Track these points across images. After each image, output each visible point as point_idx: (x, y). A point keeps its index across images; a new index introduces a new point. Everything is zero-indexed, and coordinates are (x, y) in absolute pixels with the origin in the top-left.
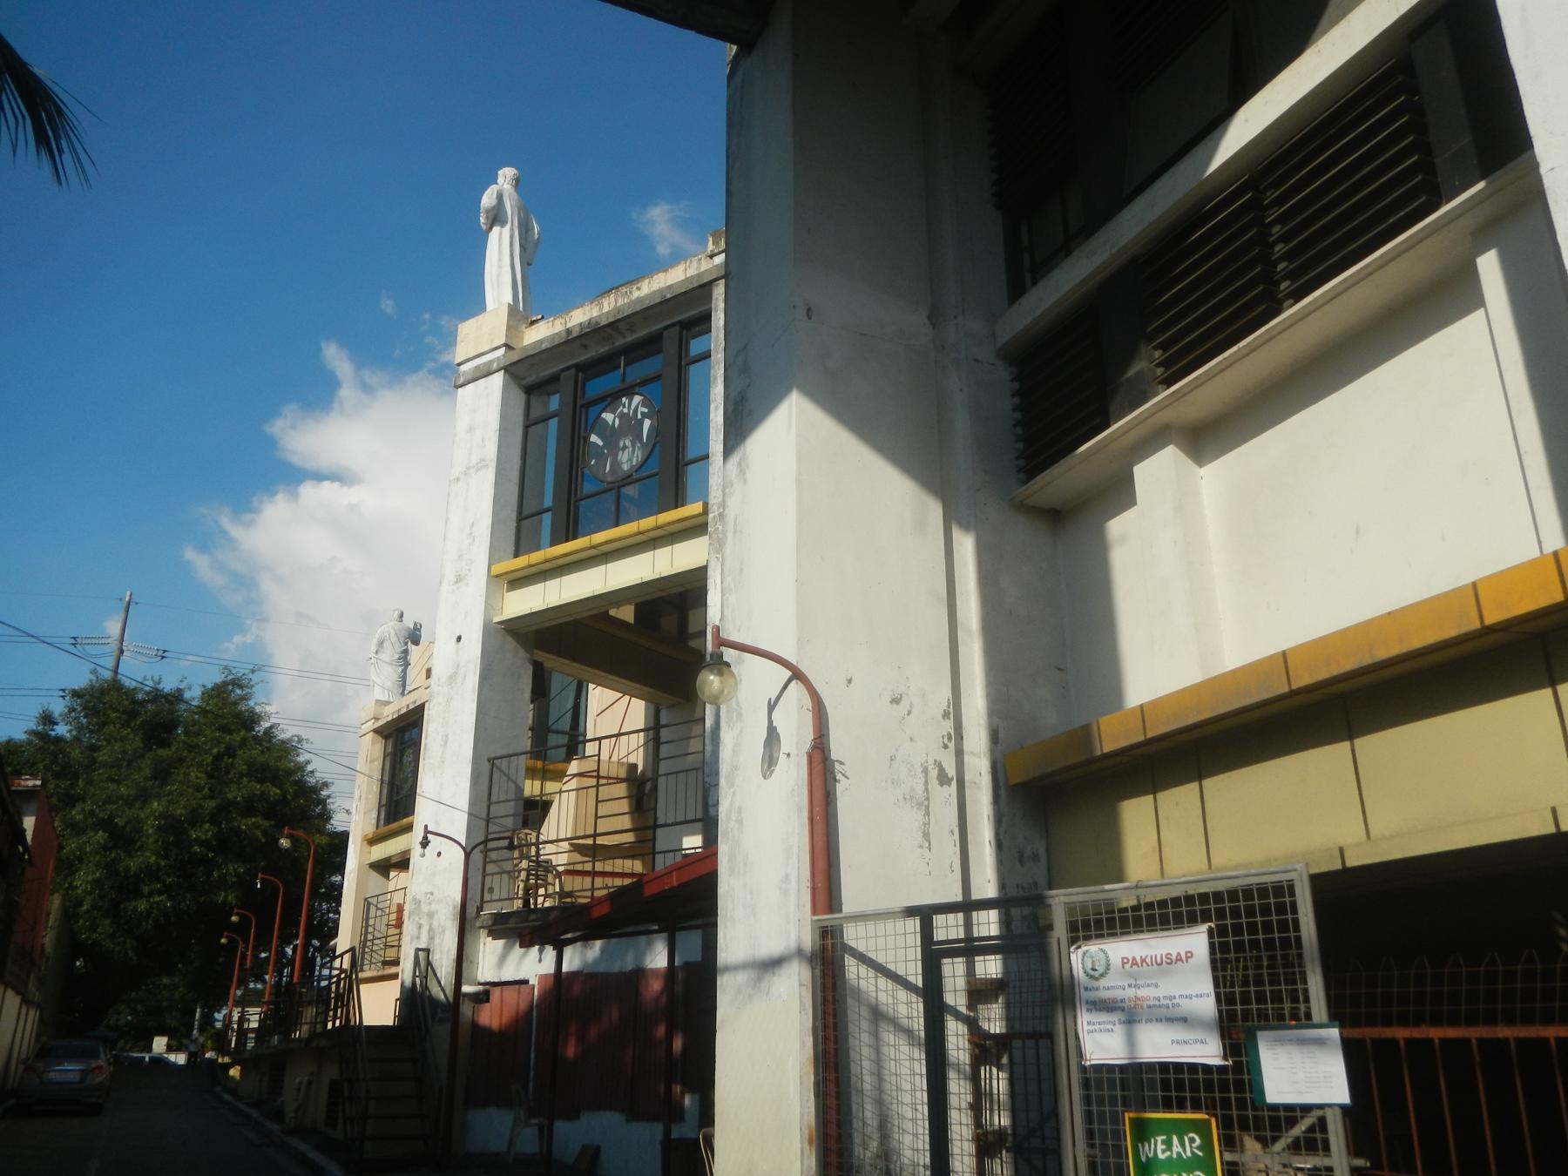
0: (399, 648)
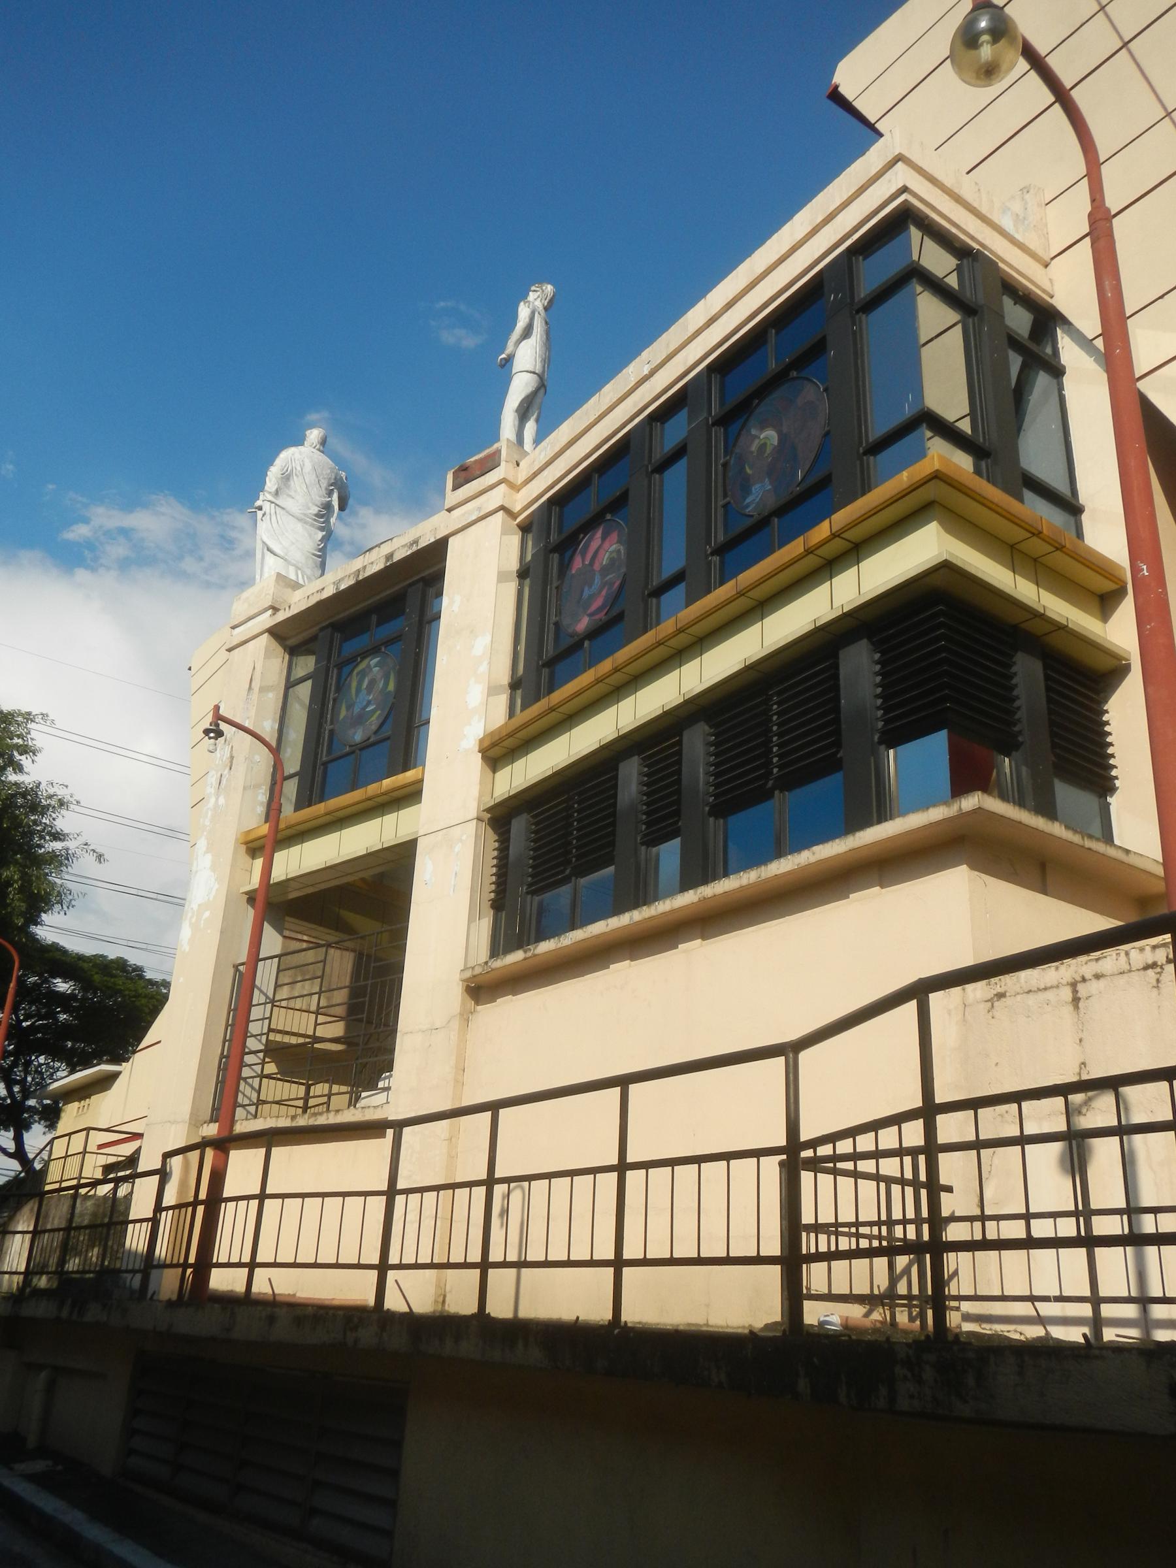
0: (318, 496)
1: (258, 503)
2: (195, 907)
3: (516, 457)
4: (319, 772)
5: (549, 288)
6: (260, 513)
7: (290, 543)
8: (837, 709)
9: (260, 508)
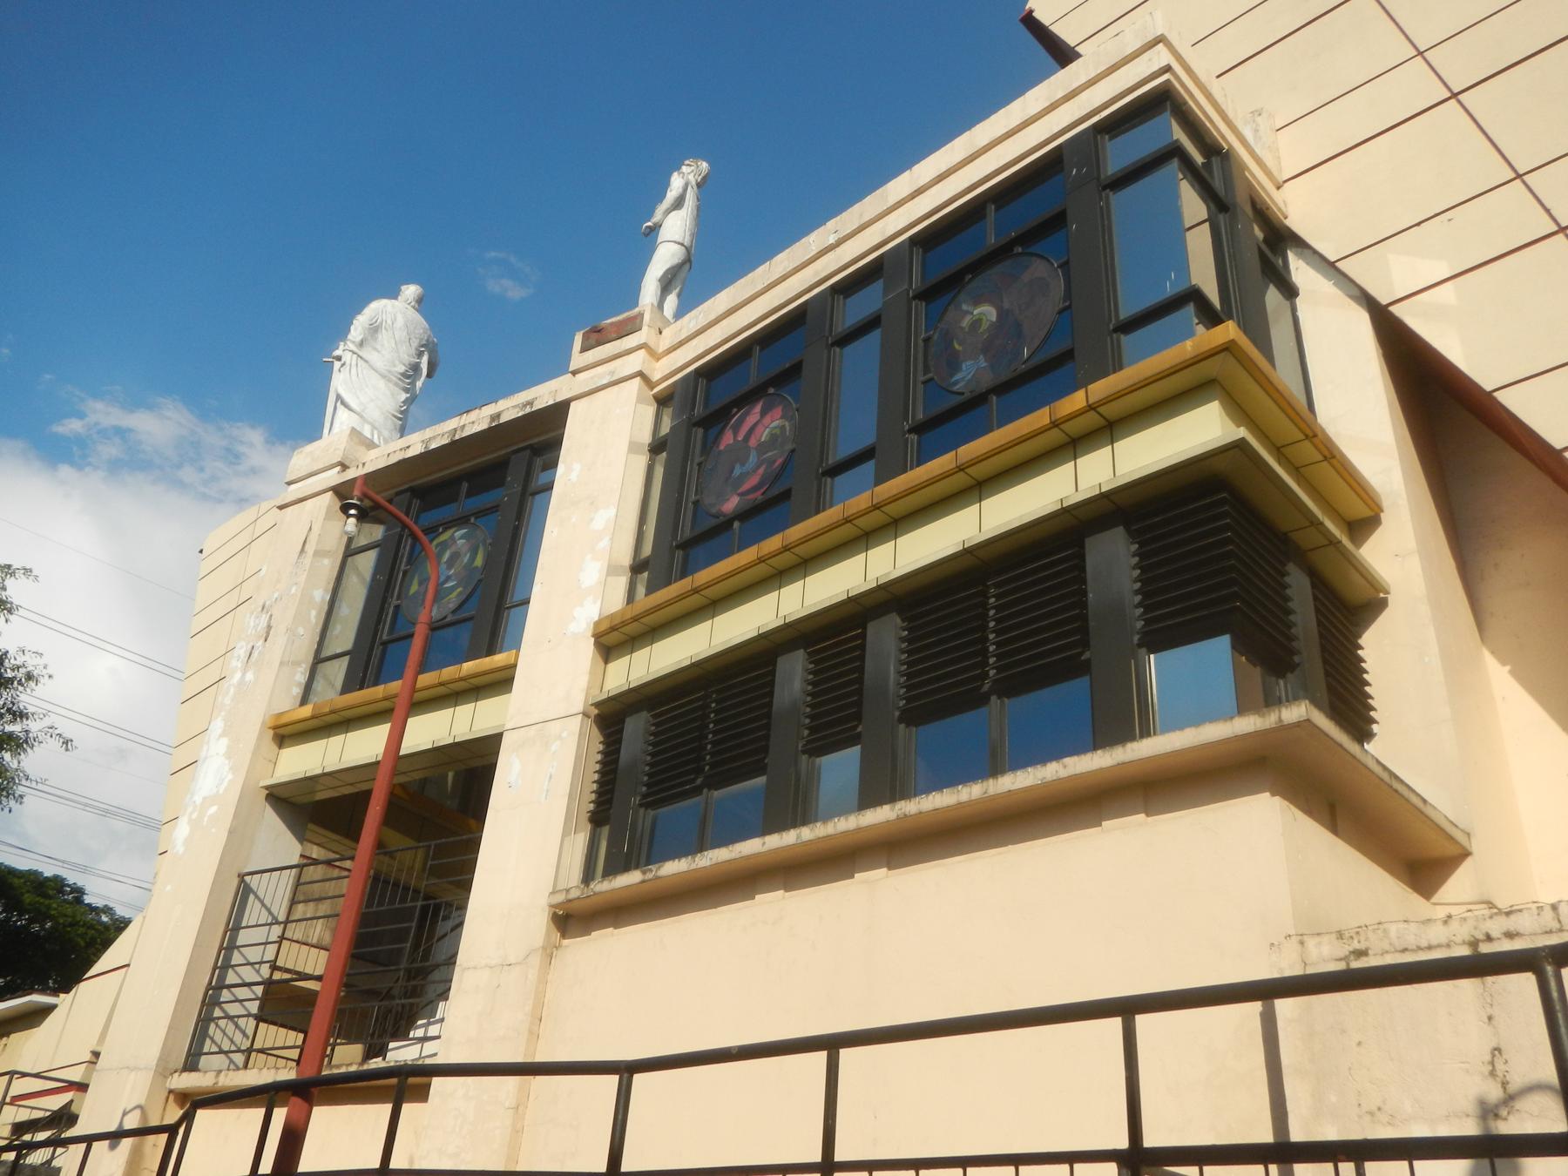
0: (406, 355)
1: (337, 353)
2: (198, 799)
3: (659, 324)
4: (377, 651)
5: (704, 165)
6: (337, 364)
7: (372, 396)
8: (1084, 605)
9: (339, 358)
